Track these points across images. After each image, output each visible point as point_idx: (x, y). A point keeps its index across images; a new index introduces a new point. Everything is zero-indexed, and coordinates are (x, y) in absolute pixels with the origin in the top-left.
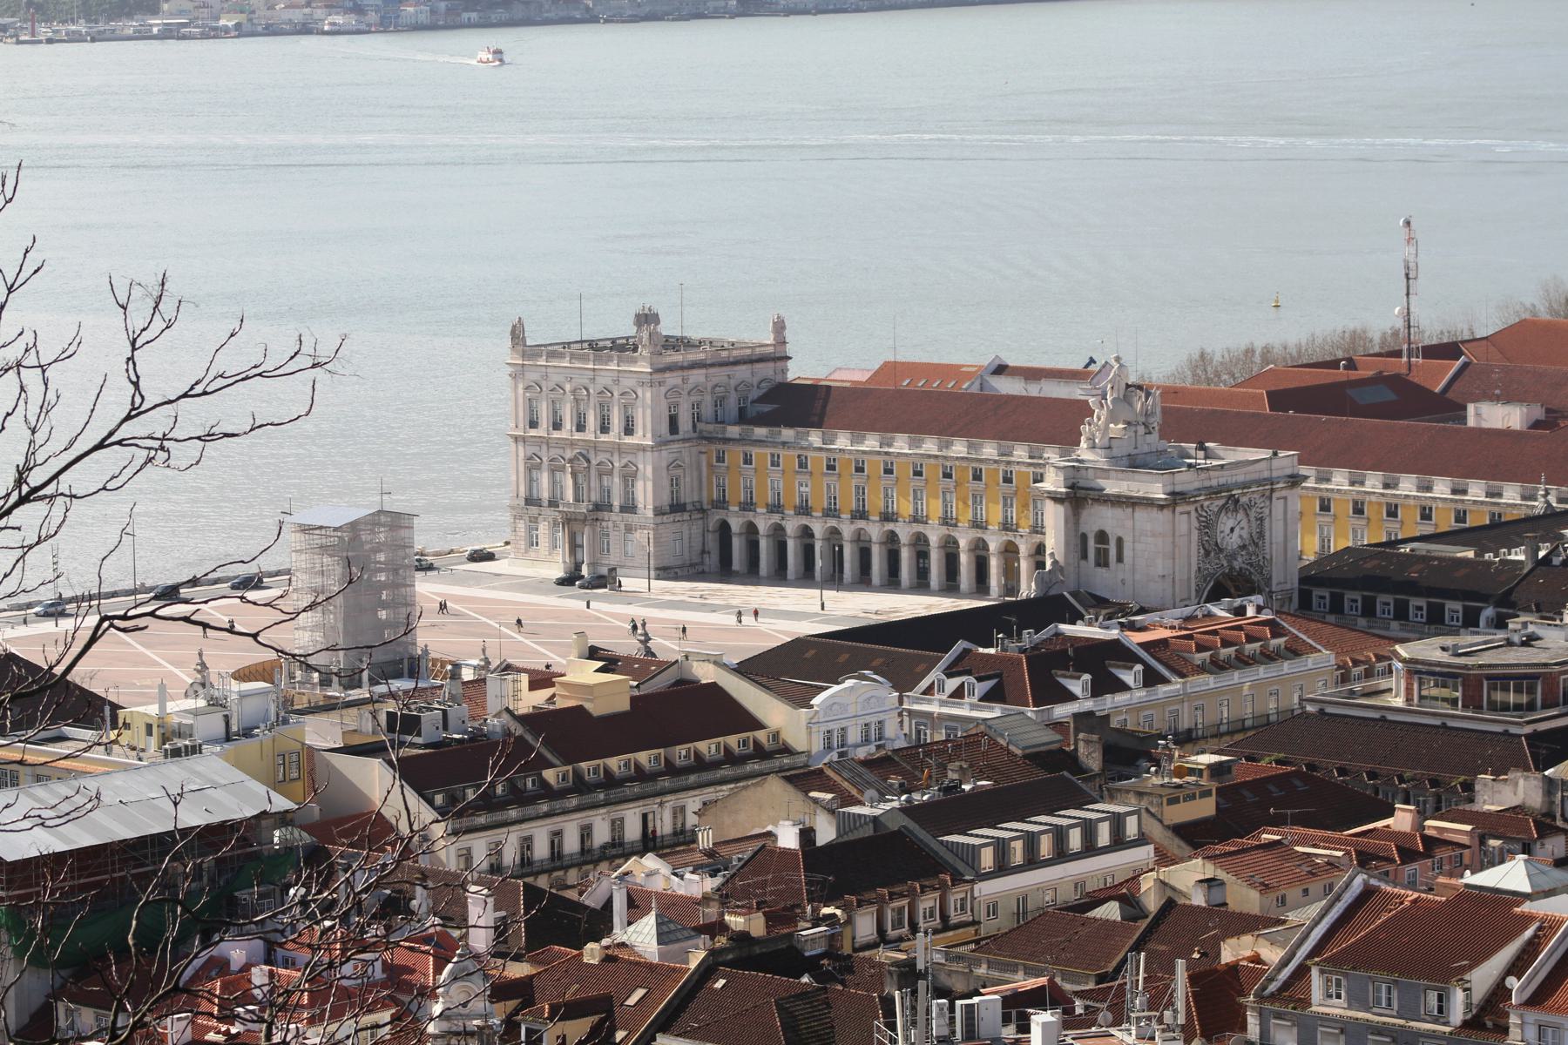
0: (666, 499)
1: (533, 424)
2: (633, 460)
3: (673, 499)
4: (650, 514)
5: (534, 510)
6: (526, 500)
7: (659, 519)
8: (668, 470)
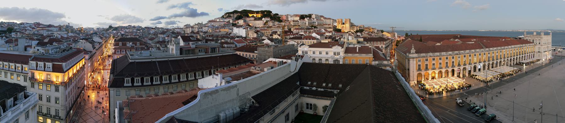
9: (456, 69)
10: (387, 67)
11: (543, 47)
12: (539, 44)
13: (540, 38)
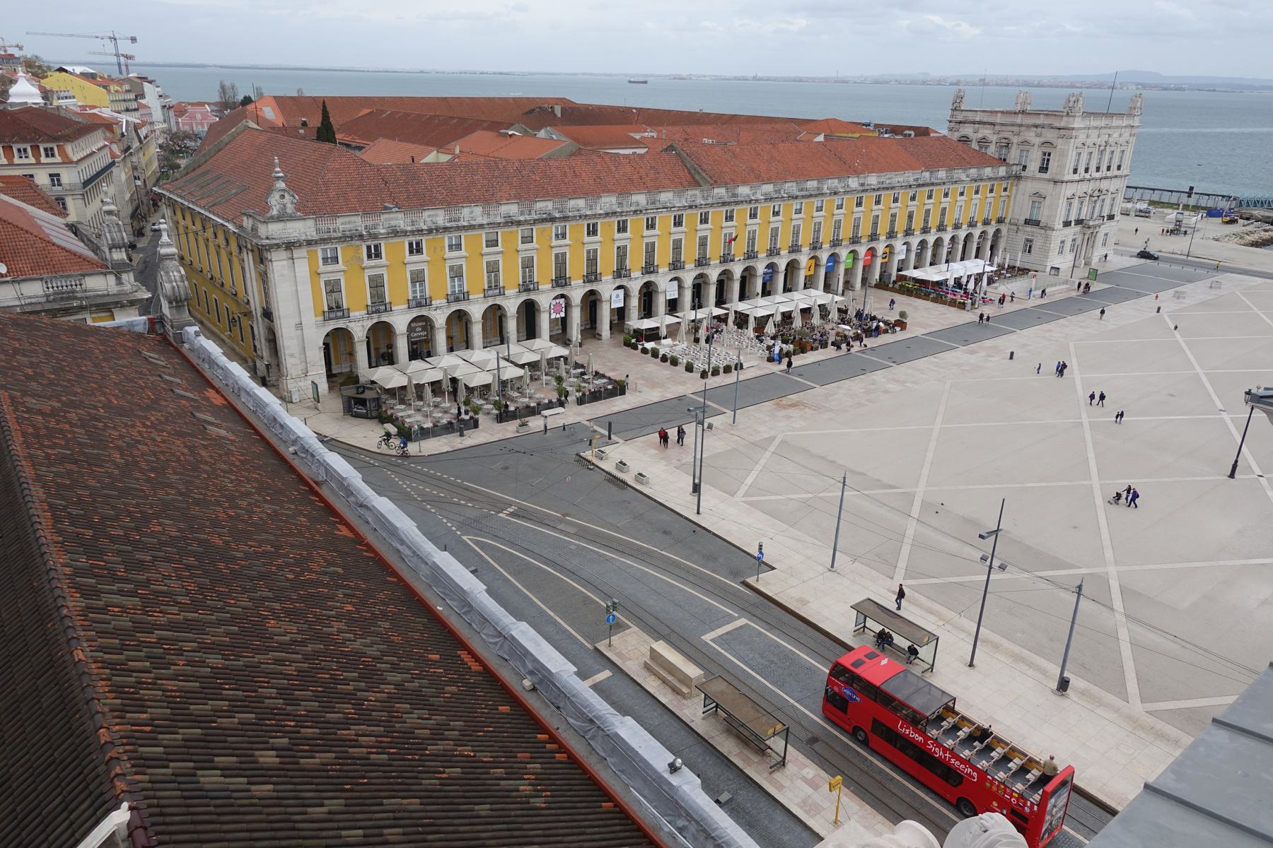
9: (545, 299)
10: (116, 312)
11: (1068, 190)
12: (1044, 169)
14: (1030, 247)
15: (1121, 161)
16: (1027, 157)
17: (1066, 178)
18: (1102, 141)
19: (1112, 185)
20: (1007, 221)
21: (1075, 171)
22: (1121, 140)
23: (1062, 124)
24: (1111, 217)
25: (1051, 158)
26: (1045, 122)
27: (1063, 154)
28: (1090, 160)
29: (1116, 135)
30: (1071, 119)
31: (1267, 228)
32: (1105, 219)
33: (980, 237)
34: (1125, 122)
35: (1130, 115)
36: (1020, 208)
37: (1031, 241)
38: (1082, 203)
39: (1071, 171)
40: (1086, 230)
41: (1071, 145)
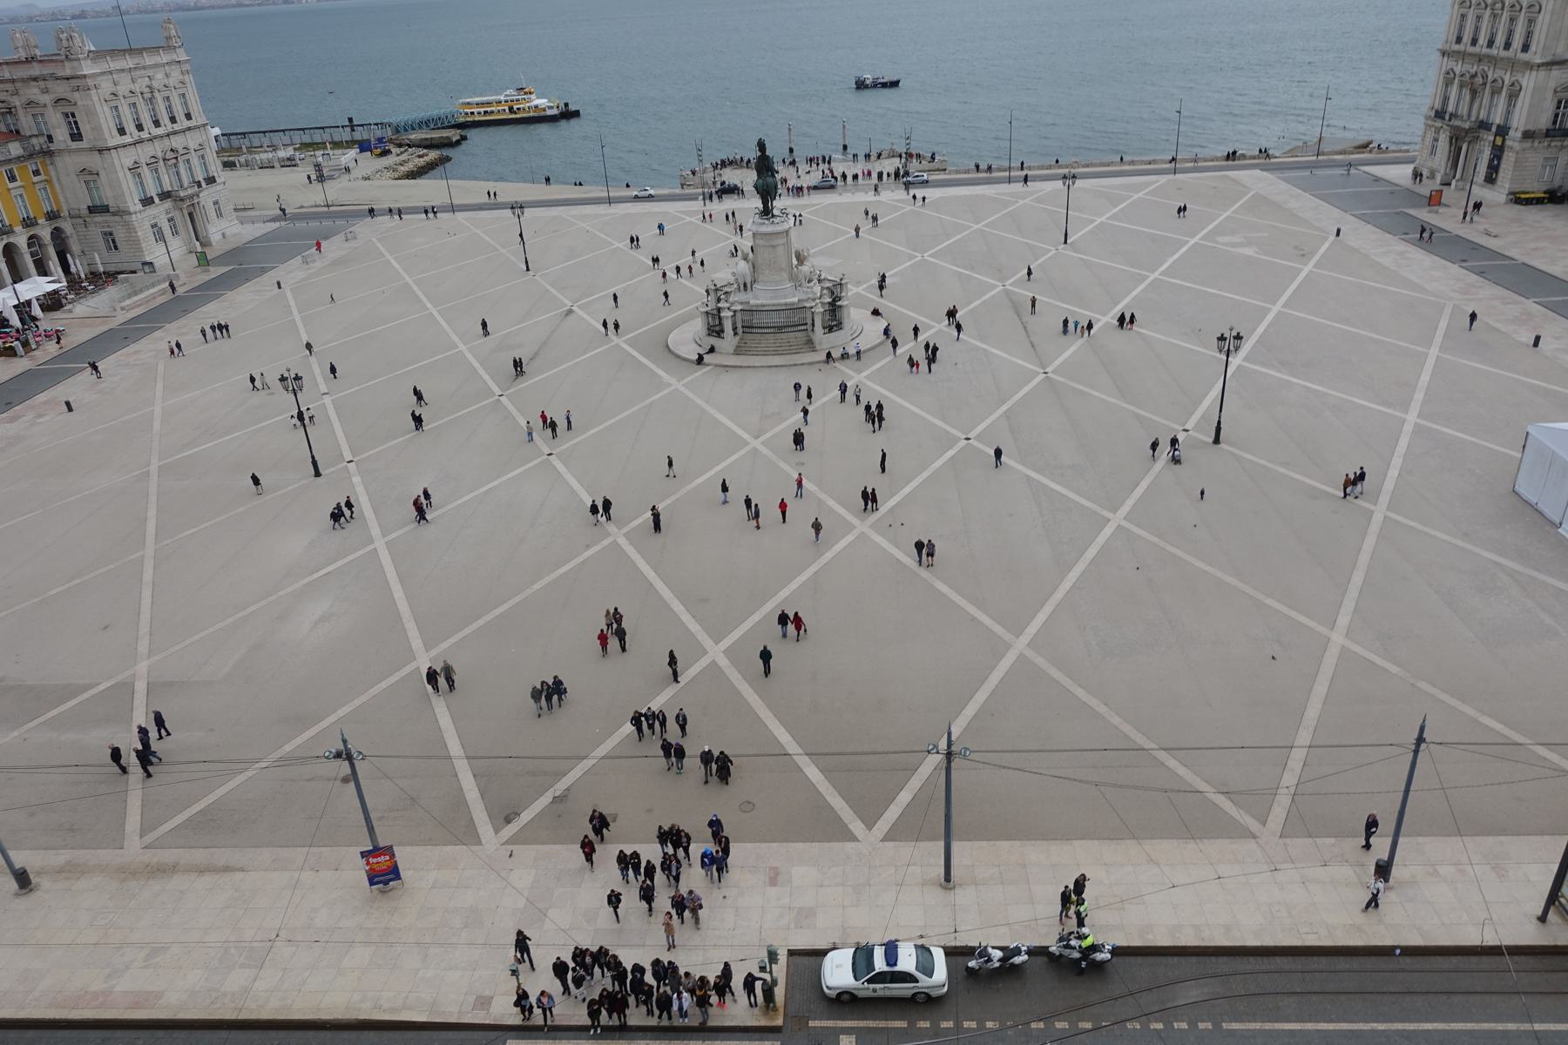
0: (1544, 121)
1: (1459, 40)
2: (1520, 80)
3: (1555, 122)
4: (1519, 135)
5: (1438, 124)
6: (1437, 112)
7: (1528, 144)
8: (1555, 92)
11: (126, 158)
12: (76, 136)
13: (61, 89)
14: (114, 241)
15: (187, 108)
16: (45, 123)
17: (111, 143)
18: (139, 86)
19: (192, 141)
20: (65, 213)
21: (122, 131)
22: (172, 81)
23: (68, 72)
24: (211, 180)
25: (77, 119)
26: (45, 72)
27: (91, 113)
28: (137, 113)
29: (160, 76)
30: (75, 63)
31: (421, 153)
32: (203, 184)
33: (29, 245)
34: (164, 58)
35: (170, 48)
36: (75, 197)
37: (111, 234)
38: (156, 170)
39: (115, 132)
40: (179, 203)
41: (95, 98)
